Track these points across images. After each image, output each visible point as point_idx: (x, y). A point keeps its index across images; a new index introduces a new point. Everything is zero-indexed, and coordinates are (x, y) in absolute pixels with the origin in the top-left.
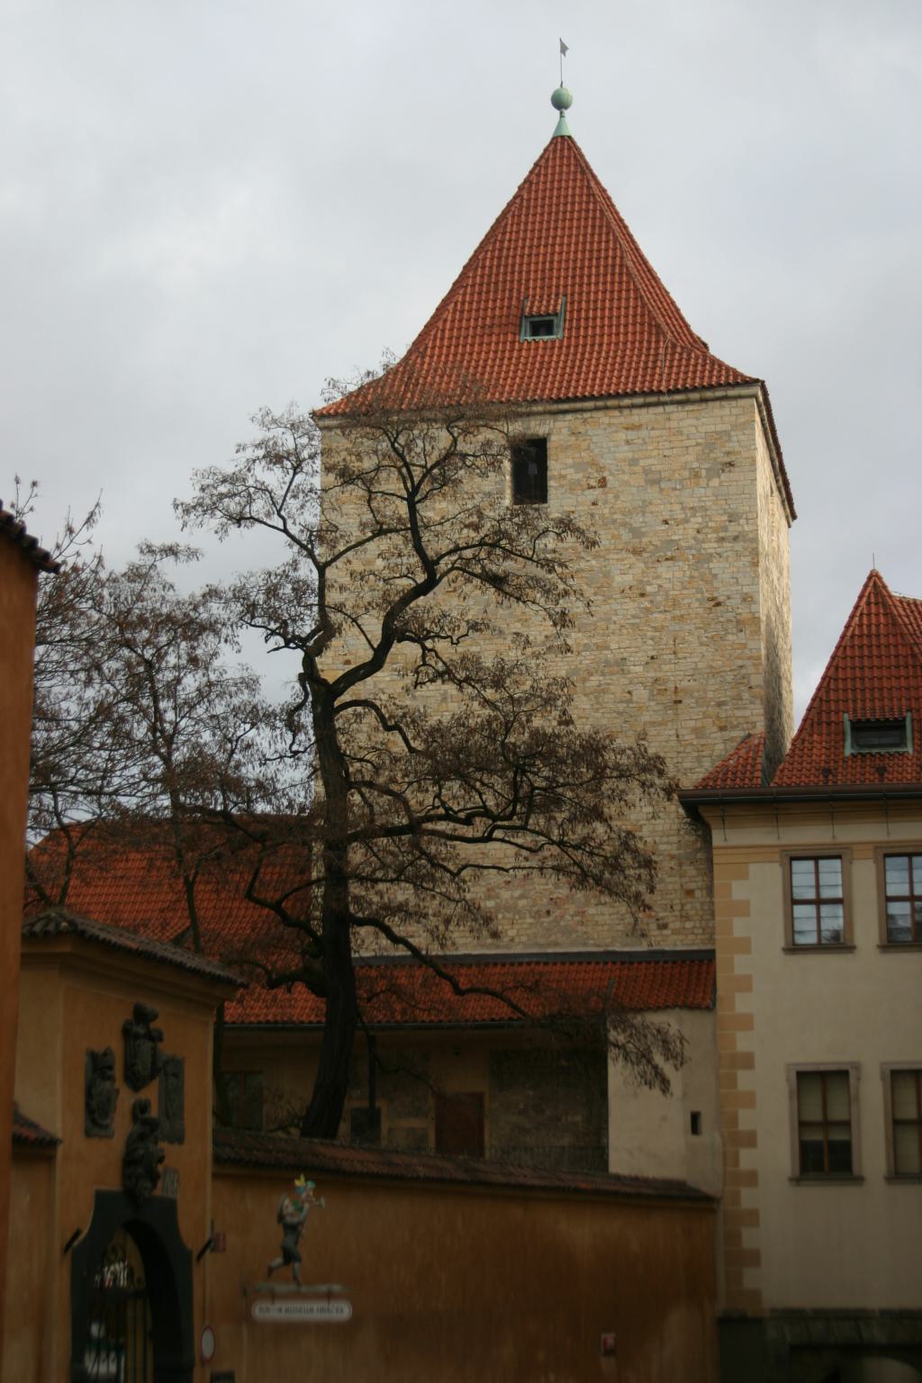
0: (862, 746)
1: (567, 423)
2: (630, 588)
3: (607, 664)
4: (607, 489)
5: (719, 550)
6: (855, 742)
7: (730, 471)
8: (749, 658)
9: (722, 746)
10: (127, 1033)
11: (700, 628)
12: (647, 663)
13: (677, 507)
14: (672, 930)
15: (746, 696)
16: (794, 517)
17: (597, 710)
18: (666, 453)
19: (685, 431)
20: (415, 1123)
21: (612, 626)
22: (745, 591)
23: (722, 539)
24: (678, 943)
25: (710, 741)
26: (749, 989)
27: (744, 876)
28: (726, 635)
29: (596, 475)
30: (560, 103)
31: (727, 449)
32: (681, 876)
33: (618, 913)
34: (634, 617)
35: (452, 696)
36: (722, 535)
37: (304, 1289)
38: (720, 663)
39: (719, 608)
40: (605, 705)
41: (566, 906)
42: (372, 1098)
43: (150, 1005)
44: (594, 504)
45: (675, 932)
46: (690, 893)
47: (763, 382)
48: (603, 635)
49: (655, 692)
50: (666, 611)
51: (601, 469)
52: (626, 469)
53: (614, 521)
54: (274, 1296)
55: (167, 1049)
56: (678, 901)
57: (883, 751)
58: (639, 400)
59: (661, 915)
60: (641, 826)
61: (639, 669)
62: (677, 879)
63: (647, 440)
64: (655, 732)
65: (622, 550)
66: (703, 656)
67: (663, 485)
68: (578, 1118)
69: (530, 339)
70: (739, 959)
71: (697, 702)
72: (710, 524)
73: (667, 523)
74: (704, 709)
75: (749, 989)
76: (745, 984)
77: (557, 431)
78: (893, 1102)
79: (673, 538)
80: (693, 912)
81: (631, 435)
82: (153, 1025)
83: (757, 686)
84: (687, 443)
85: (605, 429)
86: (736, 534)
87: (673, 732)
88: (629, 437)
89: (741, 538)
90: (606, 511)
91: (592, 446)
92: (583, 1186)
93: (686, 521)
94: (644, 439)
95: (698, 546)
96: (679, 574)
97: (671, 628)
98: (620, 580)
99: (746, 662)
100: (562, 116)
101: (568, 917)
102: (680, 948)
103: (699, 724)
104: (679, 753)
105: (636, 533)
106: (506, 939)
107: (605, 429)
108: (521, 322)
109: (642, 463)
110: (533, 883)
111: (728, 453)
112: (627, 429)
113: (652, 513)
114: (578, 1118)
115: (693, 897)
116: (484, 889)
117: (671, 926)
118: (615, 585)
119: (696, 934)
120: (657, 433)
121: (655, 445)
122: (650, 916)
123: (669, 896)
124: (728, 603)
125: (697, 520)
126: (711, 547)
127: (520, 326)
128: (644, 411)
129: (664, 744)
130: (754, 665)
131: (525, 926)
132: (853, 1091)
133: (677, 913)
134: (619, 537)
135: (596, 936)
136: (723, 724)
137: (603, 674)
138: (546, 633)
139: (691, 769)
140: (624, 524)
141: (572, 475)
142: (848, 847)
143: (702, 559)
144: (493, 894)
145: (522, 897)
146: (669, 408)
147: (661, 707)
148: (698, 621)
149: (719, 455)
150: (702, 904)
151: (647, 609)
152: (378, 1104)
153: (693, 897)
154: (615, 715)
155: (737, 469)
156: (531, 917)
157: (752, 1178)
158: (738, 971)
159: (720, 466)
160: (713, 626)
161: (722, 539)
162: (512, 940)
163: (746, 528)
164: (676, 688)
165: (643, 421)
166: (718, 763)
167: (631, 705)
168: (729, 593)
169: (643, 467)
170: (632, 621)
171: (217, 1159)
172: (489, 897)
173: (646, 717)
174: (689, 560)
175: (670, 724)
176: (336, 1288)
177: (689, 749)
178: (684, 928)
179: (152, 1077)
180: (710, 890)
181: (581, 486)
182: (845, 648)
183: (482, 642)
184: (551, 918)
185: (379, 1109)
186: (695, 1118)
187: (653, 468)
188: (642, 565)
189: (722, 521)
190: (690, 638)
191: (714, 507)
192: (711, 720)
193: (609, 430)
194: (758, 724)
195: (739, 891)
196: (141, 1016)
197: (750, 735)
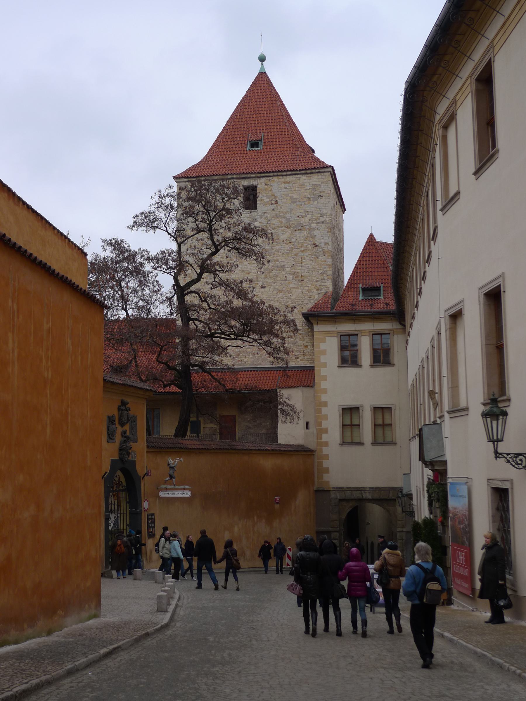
0: (365, 296)
3: (278, 267)
4: (278, 205)
5: (317, 227)
6: (364, 295)
7: (321, 199)
8: (327, 265)
9: (318, 296)
10: (119, 409)
12: (292, 267)
15: (326, 278)
16: (345, 210)
20: (212, 425)
21: (279, 254)
22: (326, 241)
23: (318, 223)
24: (302, 364)
25: (313, 294)
26: (326, 380)
27: (324, 341)
28: (319, 257)
29: (274, 199)
30: (262, 59)
31: (320, 191)
34: (287, 250)
36: (318, 221)
37: (176, 487)
39: (317, 247)
40: (277, 281)
42: (198, 418)
43: (127, 399)
44: (273, 210)
45: (301, 360)
46: (306, 346)
48: (277, 257)
51: (276, 197)
53: (280, 216)
54: (167, 489)
55: (131, 413)
56: (302, 349)
57: (372, 298)
58: (289, 173)
59: (296, 354)
61: (289, 268)
62: (302, 342)
63: (292, 187)
64: (294, 291)
66: (311, 264)
67: (298, 203)
68: (268, 423)
69: (251, 149)
70: (322, 370)
71: (309, 280)
72: (314, 217)
73: (299, 217)
74: (311, 283)
75: (326, 380)
76: (325, 378)
77: (261, 184)
78: (375, 418)
79: (301, 222)
80: (307, 353)
81: (286, 185)
82: (127, 406)
83: (330, 275)
84: (305, 189)
85: (277, 183)
86: (323, 221)
87: (301, 291)
88: (286, 186)
89: (325, 222)
90: (277, 212)
92: (268, 448)
93: (306, 216)
96: (303, 235)
97: (300, 254)
98: (282, 237)
99: (326, 266)
100: (262, 64)
104: (303, 298)
105: (288, 220)
106: (243, 363)
108: (247, 143)
109: (290, 195)
111: (320, 192)
112: (285, 183)
114: (268, 423)
117: (300, 358)
118: (280, 239)
123: (299, 348)
126: (314, 226)
127: (247, 144)
128: (291, 176)
131: (250, 358)
132: (361, 414)
133: (302, 354)
134: (281, 222)
137: (277, 271)
140: (284, 217)
141: (266, 200)
142: (360, 331)
143: (311, 230)
146: (299, 176)
147: (297, 282)
150: (310, 350)
151: (292, 248)
152: (200, 419)
155: (323, 198)
157: (326, 444)
158: (322, 374)
159: (318, 197)
160: (314, 254)
161: (318, 223)
163: (327, 219)
164: (302, 275)
166: (316, 302)
167: (286, 281)
169: (291, 197)
171: (148, 447)
174: (306, 230)
176: (187, 487)
178: (304, 359)
179: (127, 423)
180: (313, 345)
182: (360, 261)
184: (259, 355)
185: (200, 421)
186: (307, 424)
187: (294, 197)
188: (290, 232)
191: (315, 211)
194: (330, 288)
195: (323, 346)
196: (123, 403)
197: (327, 292)
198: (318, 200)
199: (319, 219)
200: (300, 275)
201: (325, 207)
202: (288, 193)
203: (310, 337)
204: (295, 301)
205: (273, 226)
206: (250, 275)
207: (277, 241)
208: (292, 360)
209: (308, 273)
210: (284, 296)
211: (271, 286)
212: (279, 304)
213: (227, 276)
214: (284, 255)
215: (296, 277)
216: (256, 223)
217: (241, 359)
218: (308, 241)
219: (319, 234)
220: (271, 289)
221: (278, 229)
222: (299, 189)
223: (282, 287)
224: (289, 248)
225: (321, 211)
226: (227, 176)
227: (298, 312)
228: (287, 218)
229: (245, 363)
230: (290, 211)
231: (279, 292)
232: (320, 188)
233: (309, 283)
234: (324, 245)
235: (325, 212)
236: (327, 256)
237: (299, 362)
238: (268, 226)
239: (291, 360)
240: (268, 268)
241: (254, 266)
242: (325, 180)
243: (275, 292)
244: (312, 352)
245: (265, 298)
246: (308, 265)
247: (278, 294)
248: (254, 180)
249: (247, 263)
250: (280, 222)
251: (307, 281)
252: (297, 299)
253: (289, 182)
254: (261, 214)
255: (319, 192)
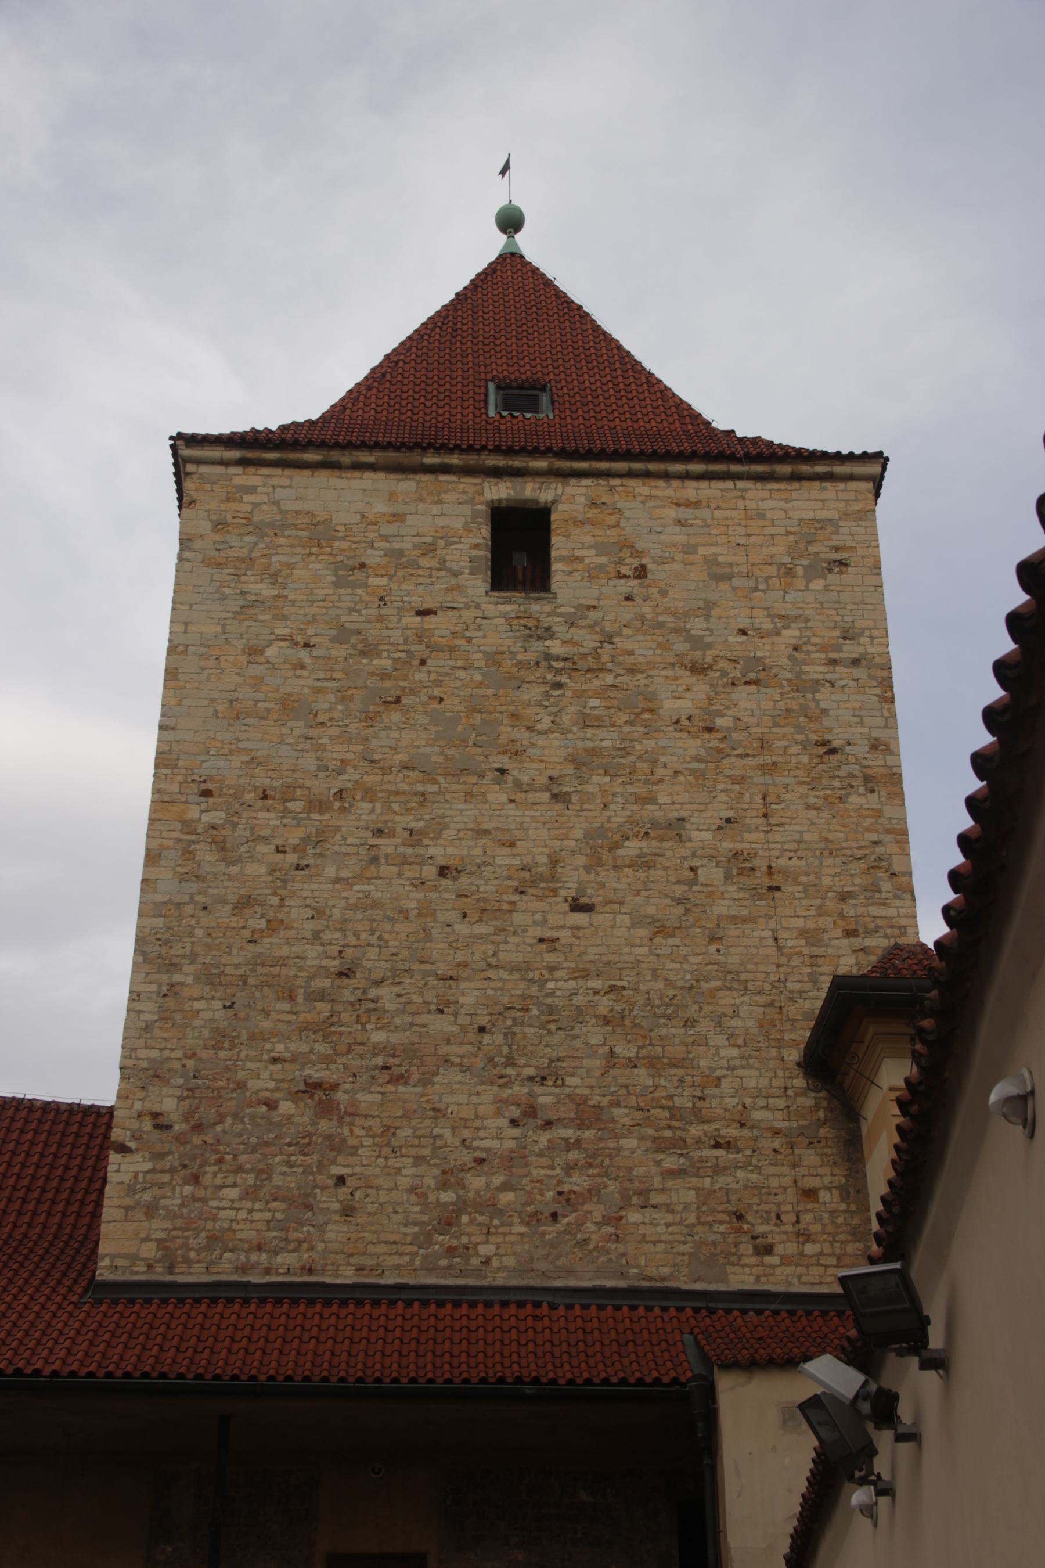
1: (584, 490)
2: (689, 718)
3: (654, 824)
4: (647, 582)
5: (828, 677)
7: (841, 573)
8: (888, 831)
9: (852, 960)
11: (804, 783)
12: (720, 828)
13: (759, 613)
14: (782, 1257)
17: (637, 893)
18: (742, 541)
19: (769, 515)
21: (660, 772)
22: (875, 734)
23: (834, 662)
24: (795, 1281)
25: (830, 951)
28: (848, 795)
32: (795, 1165)
33: (680, 1223)
34: (697, 759)
35: (387, 856)
36: (833, 655)
38: (841, 835)
39: (837, 757)
40: (650, 885)
41: (587, 1207)
44: (627, 599)
45: (785, 1261)
46: (810, 1194)
47: (887, 459)
48: (647, 782)
49: (734, 872)
50: (747, 755)
51: (639, 554)
52: (679, 557)
53: (661, 625)
59: (760, 1229)
60: (719, 1079)
61: (707, 836)
62: (785, 1170)
63: (709, 522)
64: (737, 933)
65: (673, 665)
66: (813, 824)
67: (736, 582)
71: (805, 891)
72: (815, 640)
74: (818, 902)
79: (759, 654)
81: (685, 513)
85: (643, 502)
86: (855, 655)
89: (864, 663)
90: (646, 610)
91: (623, 523)
93: (778, 634)
94: (704, 520)
95: (797, 669)
98: (670, 706)
101: (590, 1226)
102: (797, 1288)
103: (811, 924)
105: (698, 643)
106: (475, 1261)
107: (643, 502)
109: (702, 551)
110: (527, 1165)
111: (837, 549)
112: (678, 505)
113: (720, 618)
115: (817, 1202)
116: (437, 1172)
117: (779, 1249)
118: (661, 712)
119: (826, 1267)
120: (728, 513)
121: (723, 529)
122: (740, 1231)
123: (772, 1198)
124: (848, 748)
125: (791, 635)
126: (816, 671)
128: (704, 484)
129: (755, 951)
130: (897, 842)
131: (513, 1238)
133: (789, 1228)
135: (643, 1263)
136: (852, 926)
138: (550, 773)
139: (801, 992)
140: (676, 631)
141: (591, 557)
144: (452, 1180)
145: (505, 1187)
146: (741, 484)
147: (747, 896)
148: (801, 773)
149: (822, 550)
151: (719, 751)
153: (817, 1202)
154: (668, 901)
156: (523, 1222)
160: (825, 781)
161: (834, 662)
162: (487, 1261)
163: (871, 650)
164: (770, 867)
165: (701, 497)
167: (695, 888)
168: (847, 736)
170: (695, 765)
172: (444, 1186)
173: (722, 908)
174: (782, 686)
175: (761, 921)
177: (796, 961)
178: (802, 1254)
181: (608, 573)
183: (441, 779)
184: (559, 1227)
187: (720, 559)
188: (707, 688)
189: (832, 638)
190: (788, 796)
191: (818, 617)
192: (830, 919)
193: (649, 504)
198: (830, 577)
199: (838, 649)
200: (761, 864)
201: (861, 606)
202: (692, 541)
203: (827, 1150)
204: (743, 977)
205: (629, 659)
206: (514, 851)
207: (645, 720)
208: (740, 1257)
209: (800, 858)
210: (684, 950)
211: (622, 903)
212: (660, 985)
213: (401, 849)
214: (682, 778)
215: (741, 872)
216: (548, 643)
217: (464, 1240)
218: (792, 730)
219: (842, 705)
220: (624, 920)
221: (651, 673)
222: (742, 531)
223: (680, 909)
224: (702, 752)
225: (846, 619)
226: (423, 456)
227: (761, 1026)
228: (692, 632)
229: (487, 1261)
230: (708, 608)
231: (662, 930)
232: (832, 533)
233: (804, 902)
234: (867, 749)
235: (860, 624)
236: (883, 793)
237: (778, 1271)
238: (605, 659)
239: (733, 1259)
240: (607, 826)
241: (538, 813)
242: (857, 508)
243: (644, 932)
244: (840, 1220)
245: (585, 958)
246: (797, 828)
247: (658, 940)
248: (537, 485)
249: (504, 798)
250: (660, 645)
251: (797, 895)
252: (750, 967)
253: (696, 504)
254: (573, 610)
255: (832, 548)
